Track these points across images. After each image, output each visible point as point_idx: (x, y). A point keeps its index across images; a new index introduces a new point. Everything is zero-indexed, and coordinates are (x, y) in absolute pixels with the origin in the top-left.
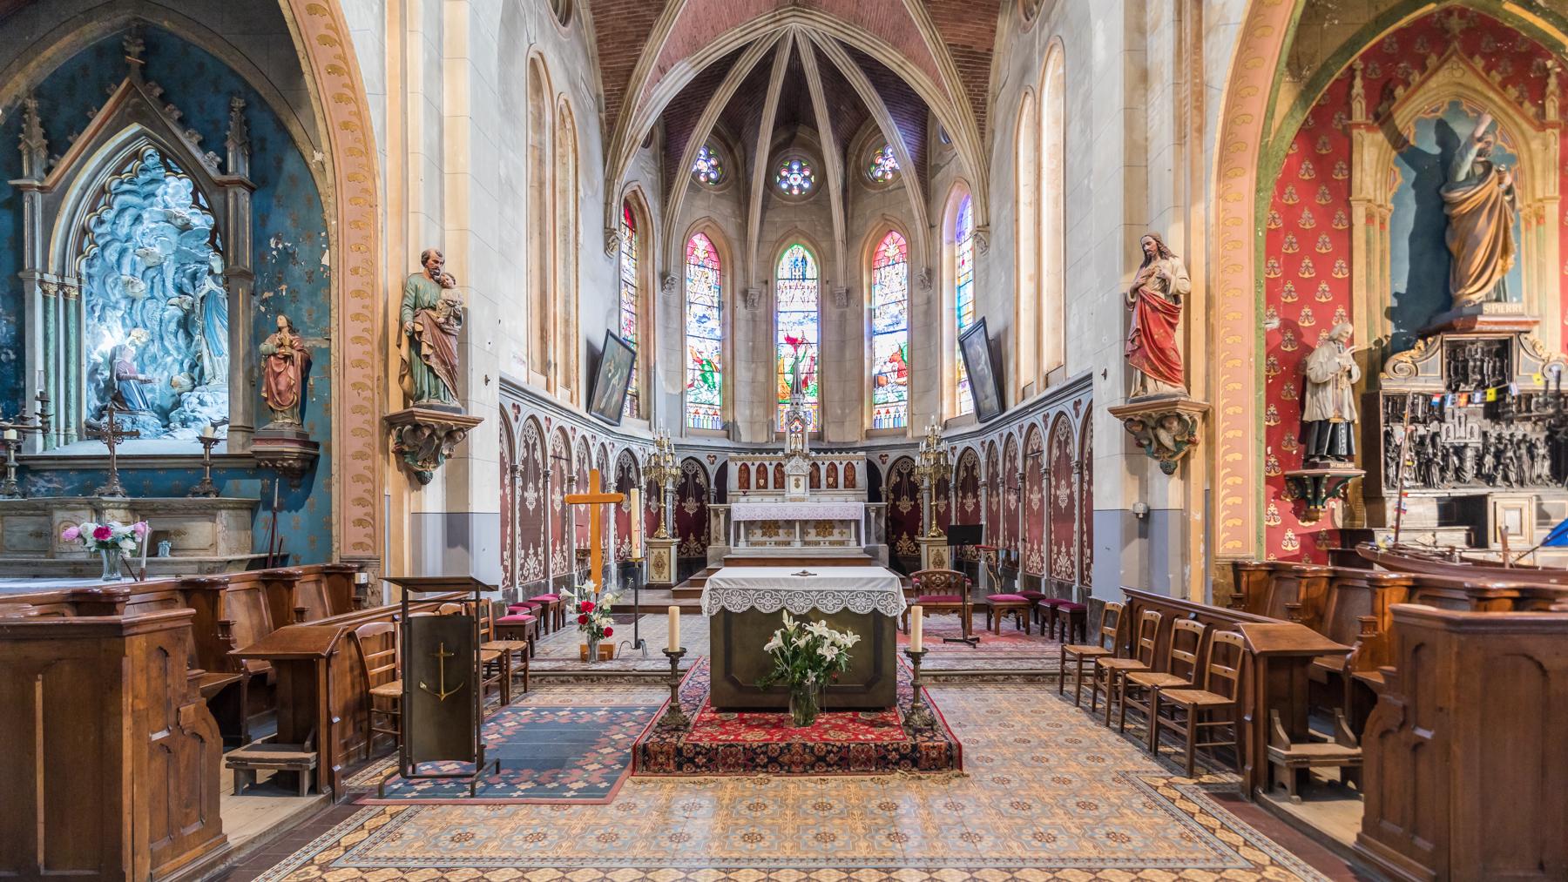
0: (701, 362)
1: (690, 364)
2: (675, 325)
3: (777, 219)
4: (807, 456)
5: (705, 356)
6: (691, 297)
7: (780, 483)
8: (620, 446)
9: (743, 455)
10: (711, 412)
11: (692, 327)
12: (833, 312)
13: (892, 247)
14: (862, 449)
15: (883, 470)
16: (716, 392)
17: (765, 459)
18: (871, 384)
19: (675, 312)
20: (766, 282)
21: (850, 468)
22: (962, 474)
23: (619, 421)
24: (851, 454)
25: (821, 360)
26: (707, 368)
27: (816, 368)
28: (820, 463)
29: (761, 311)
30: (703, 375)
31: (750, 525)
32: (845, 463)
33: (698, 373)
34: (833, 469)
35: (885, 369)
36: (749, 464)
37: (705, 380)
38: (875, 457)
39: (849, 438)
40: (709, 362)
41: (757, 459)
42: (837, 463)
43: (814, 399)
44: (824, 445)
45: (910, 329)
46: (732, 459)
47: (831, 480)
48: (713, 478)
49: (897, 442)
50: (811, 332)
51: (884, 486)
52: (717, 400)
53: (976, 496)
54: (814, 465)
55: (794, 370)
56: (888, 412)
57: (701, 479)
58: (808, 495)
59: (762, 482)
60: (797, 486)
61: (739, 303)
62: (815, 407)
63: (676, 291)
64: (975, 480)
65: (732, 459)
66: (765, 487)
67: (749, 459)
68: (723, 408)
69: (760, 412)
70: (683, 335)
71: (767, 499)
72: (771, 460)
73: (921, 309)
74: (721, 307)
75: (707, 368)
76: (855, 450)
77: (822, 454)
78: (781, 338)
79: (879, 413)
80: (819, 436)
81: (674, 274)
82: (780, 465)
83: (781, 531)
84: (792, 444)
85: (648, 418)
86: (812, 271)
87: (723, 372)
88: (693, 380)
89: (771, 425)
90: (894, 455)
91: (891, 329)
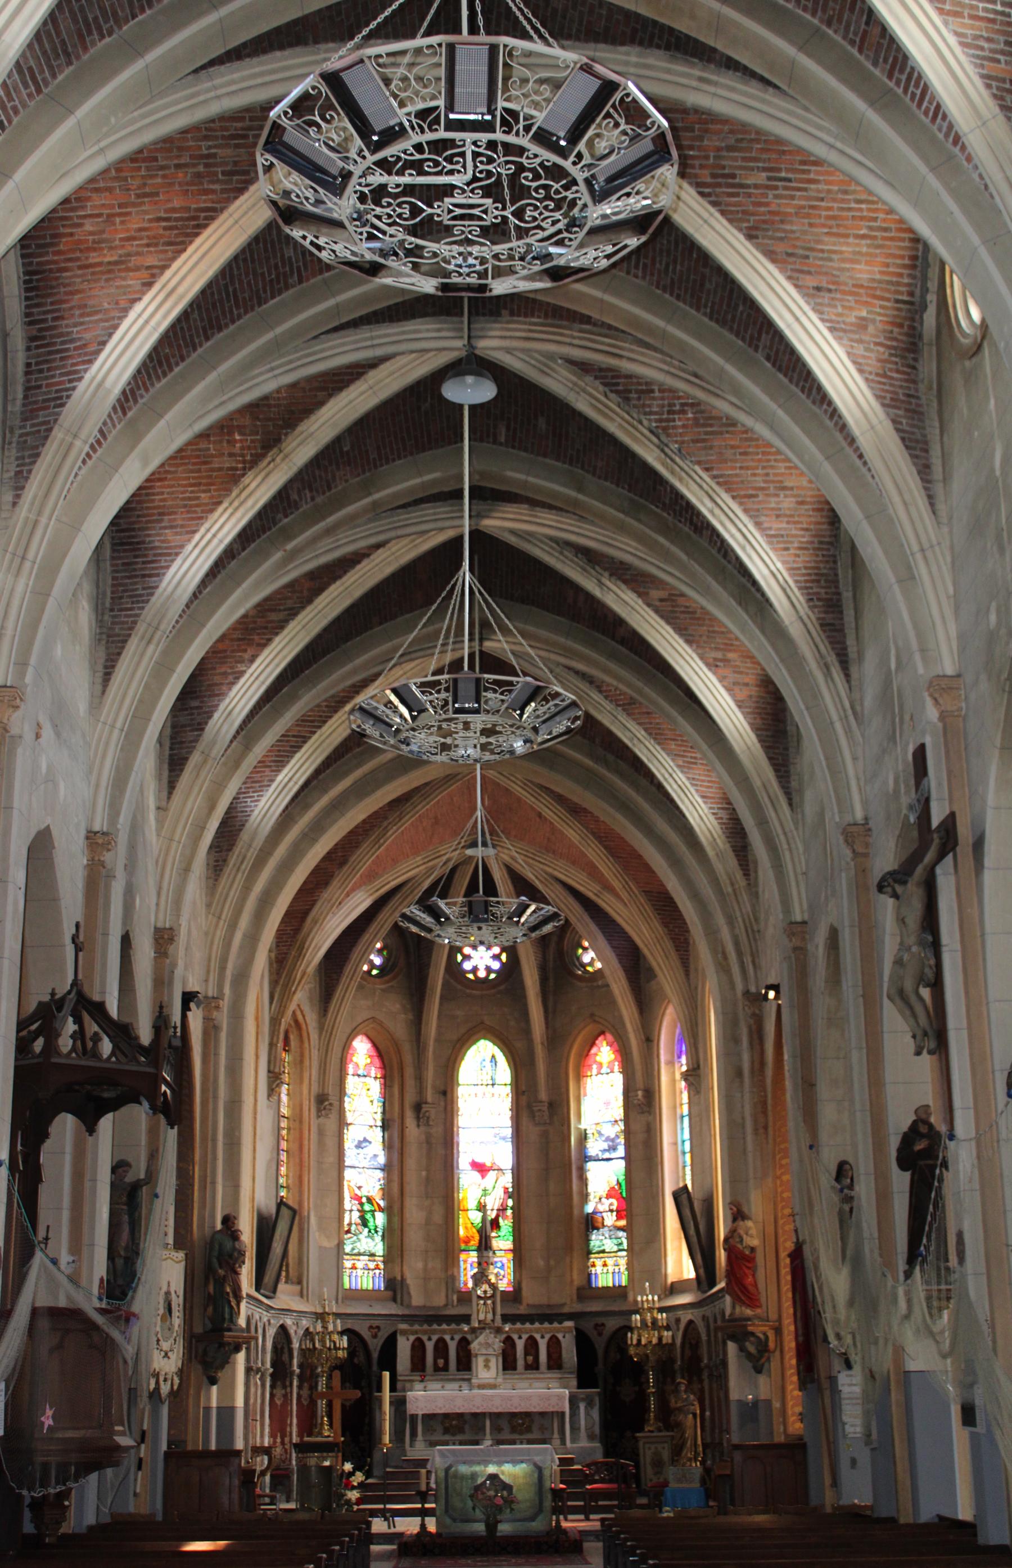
0: (358, 1199)
1: (348, 1204)
2: (331, 1159)
3: (459, 1013)
4: (498, 1331)
5: (363, 1193)
6: (350, 1117)
7: (465, 1363)
8: (276, 1323)
9: (417, 1327)
10: (372, 1265)
11: (351, 1156)
12: (532, 1132)
13: (605, 1053)
14: (570, 1316)
15: (600, 1344)
16: (378, 1238)
17: (444, 1332)
18: (583, 1226)
19: (331, 1142)
20: (444, 1093)
21: (554, 1344)
22: (688, 1353)
23: (274, 1290)
24: (556, 1325)
25: (517, 1192)
26: (367, 1207)
27: (510, 1202)
28: (515, 1337)
29: (437, 1130)
30: (362, 1218)
31: (429, 1418)
32: (547, 1336)
33: (356, 1215)
34: (532, 1345)
35: (601, 1208)
36: (425, 1338)
37: (364, 1223)
38: (588, 1326)
39: (556, 1300)
40: (370, 1200)
41: (434, 1332)
42: (538, 1336)
43: (508, 1244)
44: (522, 1310)
45: (628, 1158)
46: (404, 1333)
47: (530, 1358)
48: (375, 1355)
49: (615, 1307)
50: (504, 1156)
51: (600, 1365)
52: (378, 1247)
53: (701, 1381)
54: (509, 1343)
55: (482, 1208)
56: (605, 1265)
57: (360, 1359)
58: (500, 1380)
59: (441, 1362)
60: (487, 1366)
61: (410, 1122)
62: (510, 1256)
63: (334, 1116)
64: (699, 1359)
65: (404, 1333)
66: (446, 1368)
67: (425, 1332)
68: (388, 1259)
69: (436, 1264)
70: (340, 1165)
71: (449, 1385)
72: (453, 1333)
73: (641, 1137)
74: (385, 1126)
75: (367, 1207)
76: (561, 1317)
77: (518, 1325)
78: (463, 1162)
79: (594, 1265)
80: (514, 1296)
81: (331, 1090)
82: (464, 1344)
83: (467, 1427)
84: (481, 1313)
85: (299, 1282)
86: (504, 1072)
87: (388, 1210)
88: (350, 1224)
89: (451, 1279)
90: (612, 1324)
91: (607, 1155)
